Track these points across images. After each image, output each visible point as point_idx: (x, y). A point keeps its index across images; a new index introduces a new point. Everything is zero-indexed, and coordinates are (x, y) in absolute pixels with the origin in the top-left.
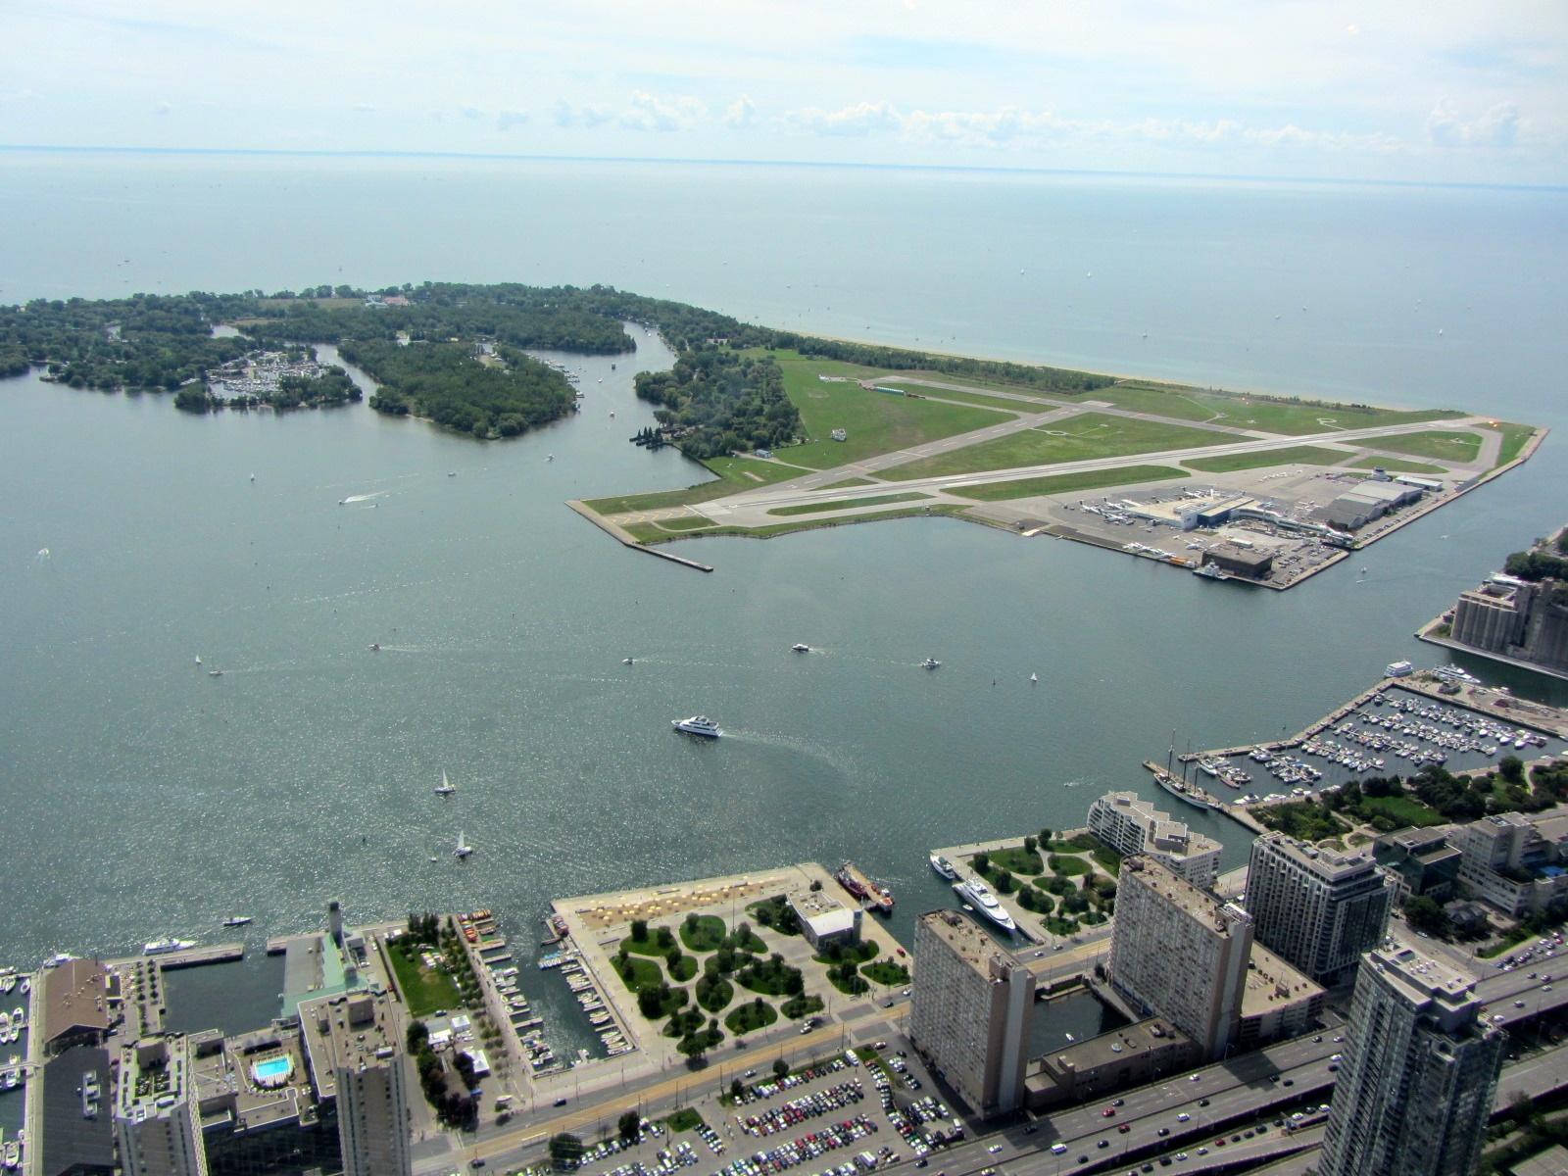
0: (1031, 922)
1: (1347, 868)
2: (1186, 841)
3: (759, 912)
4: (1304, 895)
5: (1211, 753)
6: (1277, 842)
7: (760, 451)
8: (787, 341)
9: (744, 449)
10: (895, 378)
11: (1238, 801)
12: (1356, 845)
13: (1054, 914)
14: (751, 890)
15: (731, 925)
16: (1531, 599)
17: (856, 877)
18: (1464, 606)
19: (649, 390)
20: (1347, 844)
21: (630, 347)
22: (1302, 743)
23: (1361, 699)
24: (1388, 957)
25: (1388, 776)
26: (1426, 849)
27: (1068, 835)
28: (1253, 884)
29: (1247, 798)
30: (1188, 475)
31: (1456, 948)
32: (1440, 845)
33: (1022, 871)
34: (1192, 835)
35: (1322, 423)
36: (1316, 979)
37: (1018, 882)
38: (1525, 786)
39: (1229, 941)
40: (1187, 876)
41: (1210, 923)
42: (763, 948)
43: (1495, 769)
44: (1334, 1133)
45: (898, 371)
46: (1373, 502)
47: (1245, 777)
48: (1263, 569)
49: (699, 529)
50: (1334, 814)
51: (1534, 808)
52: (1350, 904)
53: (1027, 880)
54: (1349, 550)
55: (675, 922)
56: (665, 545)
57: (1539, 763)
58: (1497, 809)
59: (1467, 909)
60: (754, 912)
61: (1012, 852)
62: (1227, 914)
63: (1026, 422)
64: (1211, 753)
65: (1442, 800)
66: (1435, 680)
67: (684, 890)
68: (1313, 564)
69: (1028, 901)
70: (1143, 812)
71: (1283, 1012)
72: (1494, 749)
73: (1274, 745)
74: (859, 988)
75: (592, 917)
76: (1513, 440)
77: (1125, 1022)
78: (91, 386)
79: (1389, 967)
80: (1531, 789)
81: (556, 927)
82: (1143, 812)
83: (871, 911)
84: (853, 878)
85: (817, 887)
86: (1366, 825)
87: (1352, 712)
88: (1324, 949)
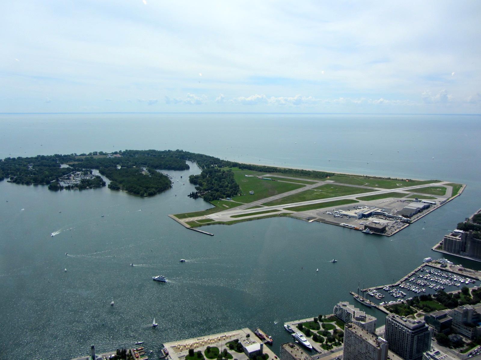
0: (317, 346)
1: (416, 324)
2: (365, 317)
3: (230, 345)
4: (404, 334)
5: (371, 289)
6: (394, 317)
7: (228, 198)
8: (235, 165)
9: (223, 198)
10: (268, 175)
11: (381, 304)
12: (419, 317)
13: (324, 343)
14: (227, 338)
15: (221, 350)
16: (466, 237)
17: (261, 332)
18: (446, 240)
19: (193, 180)
20: (416, 317)
21: (188, 168)
22: (399, 284)
23: (416, 270)
24: (432, 354)
25: (427, 294)
27: (327, 316)
28: (387, 330)
29: (383, 303)
30: (358, 202)
31: (453, 350)
32: (445, 316)
33: (313, 329)
34: (367, 315)
35: (398, 185)
37: (313, 333)
38: (470, 296)
39: (381, 350)
40: (366, 328)
41: (374, 344)
43: (460, 291)
45: (270, 173)
46: (415, 208)
47: (382, 296)
48: (383, 230)
49: (210, 222)
50: (411, 307)
51: (474, 303)
52: (418, 337)
53: (315, 332)
54: (409, 223)
55: (202, 349)
56: (199, 228)
57: (473, 288)
58: (462, 304)
59: (456, 337)
60: (228, 345)
62: (379, 341)
63: (308, 187)
64: (371, 289)
65: (445, 301)
66: (439, 263)
67: (206, 338)
68: (398, 228)
69: (316, 339)
70: (351, 308)
72: (459, 284)
73: (391, 285)
76: (456, 189)
78: (23, 183)
80: (472, 297)
81: (164, 352)
82: (351, 308)
83: (265, 343)
84: (260, 333)
85: (248, 336)
86: (422, 310)
87: (414, 274)
88: (411, 351)
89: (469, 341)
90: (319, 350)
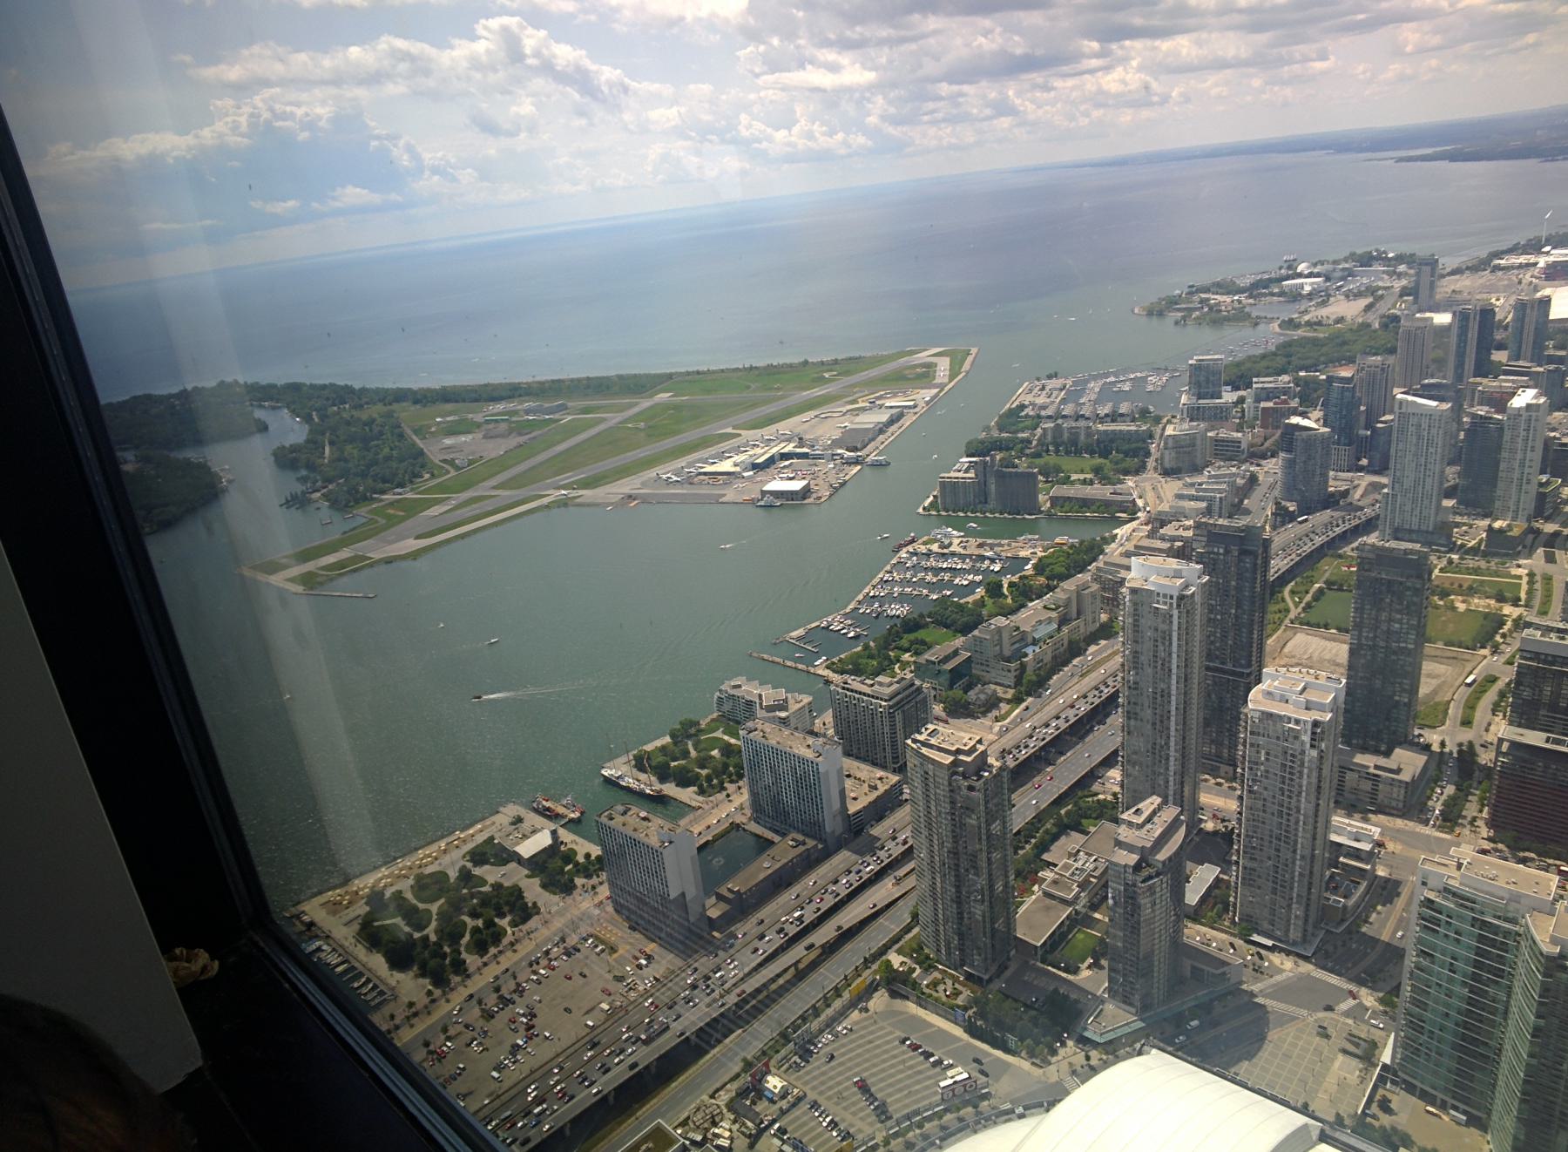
1: (895, 686)
2: (786, 700)
8: (400, 396)
9: (383, 492)
18: (943, 485)
24: (921, 738)
26: (946, 659)
32: (956, 653)
36: (894, 771)
42: (484, 882)
44: (920, 876)
58: (992, 616)
59: (982, 692)
61: (663, 749)
65: (954, 622)
66: (935, 541)
69: (684, 780)
71: (875, 801)
74: (567, 888)
75: (335, 907)
76: (957, 358)
77: (772, 843)
79: (924, 744)
80: (1009, 600)
89: (1011, 692)
90: (694, 804)
